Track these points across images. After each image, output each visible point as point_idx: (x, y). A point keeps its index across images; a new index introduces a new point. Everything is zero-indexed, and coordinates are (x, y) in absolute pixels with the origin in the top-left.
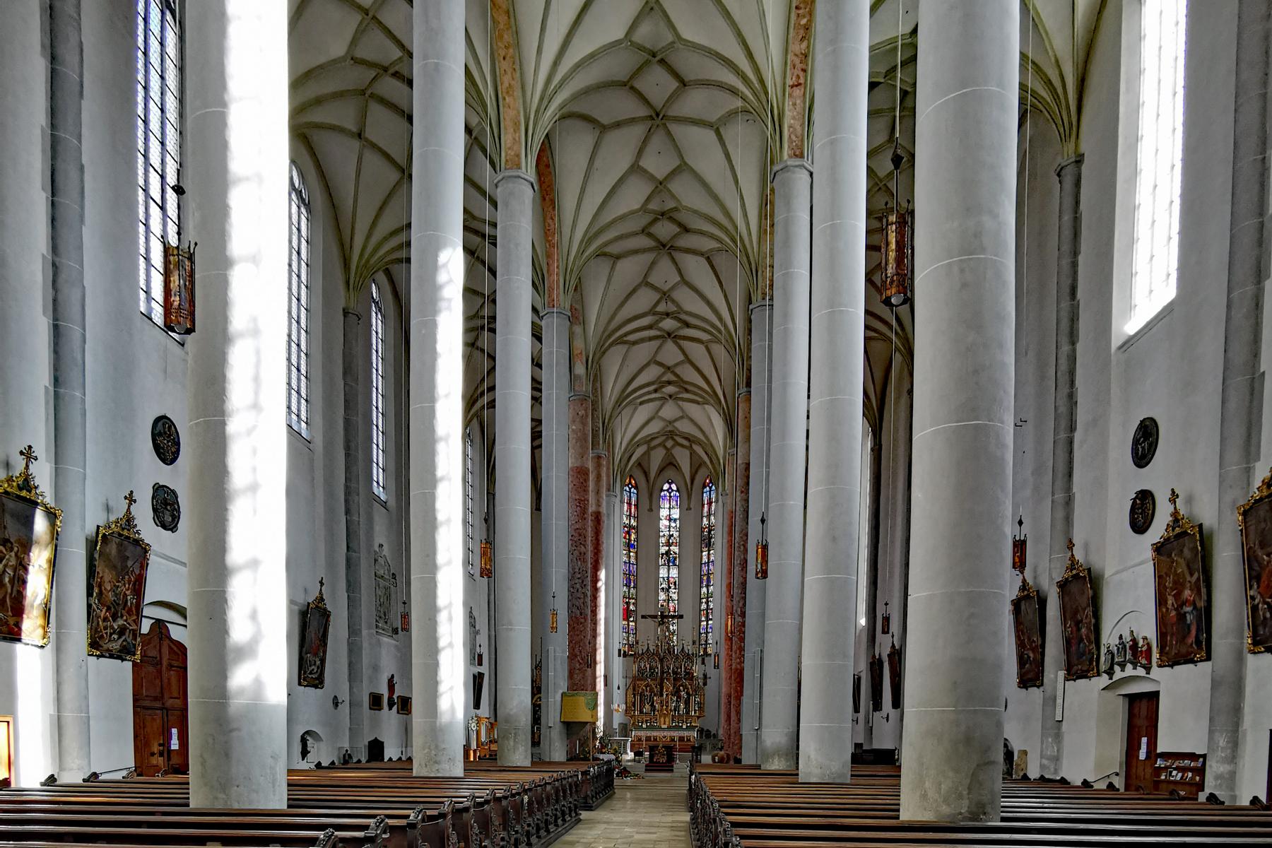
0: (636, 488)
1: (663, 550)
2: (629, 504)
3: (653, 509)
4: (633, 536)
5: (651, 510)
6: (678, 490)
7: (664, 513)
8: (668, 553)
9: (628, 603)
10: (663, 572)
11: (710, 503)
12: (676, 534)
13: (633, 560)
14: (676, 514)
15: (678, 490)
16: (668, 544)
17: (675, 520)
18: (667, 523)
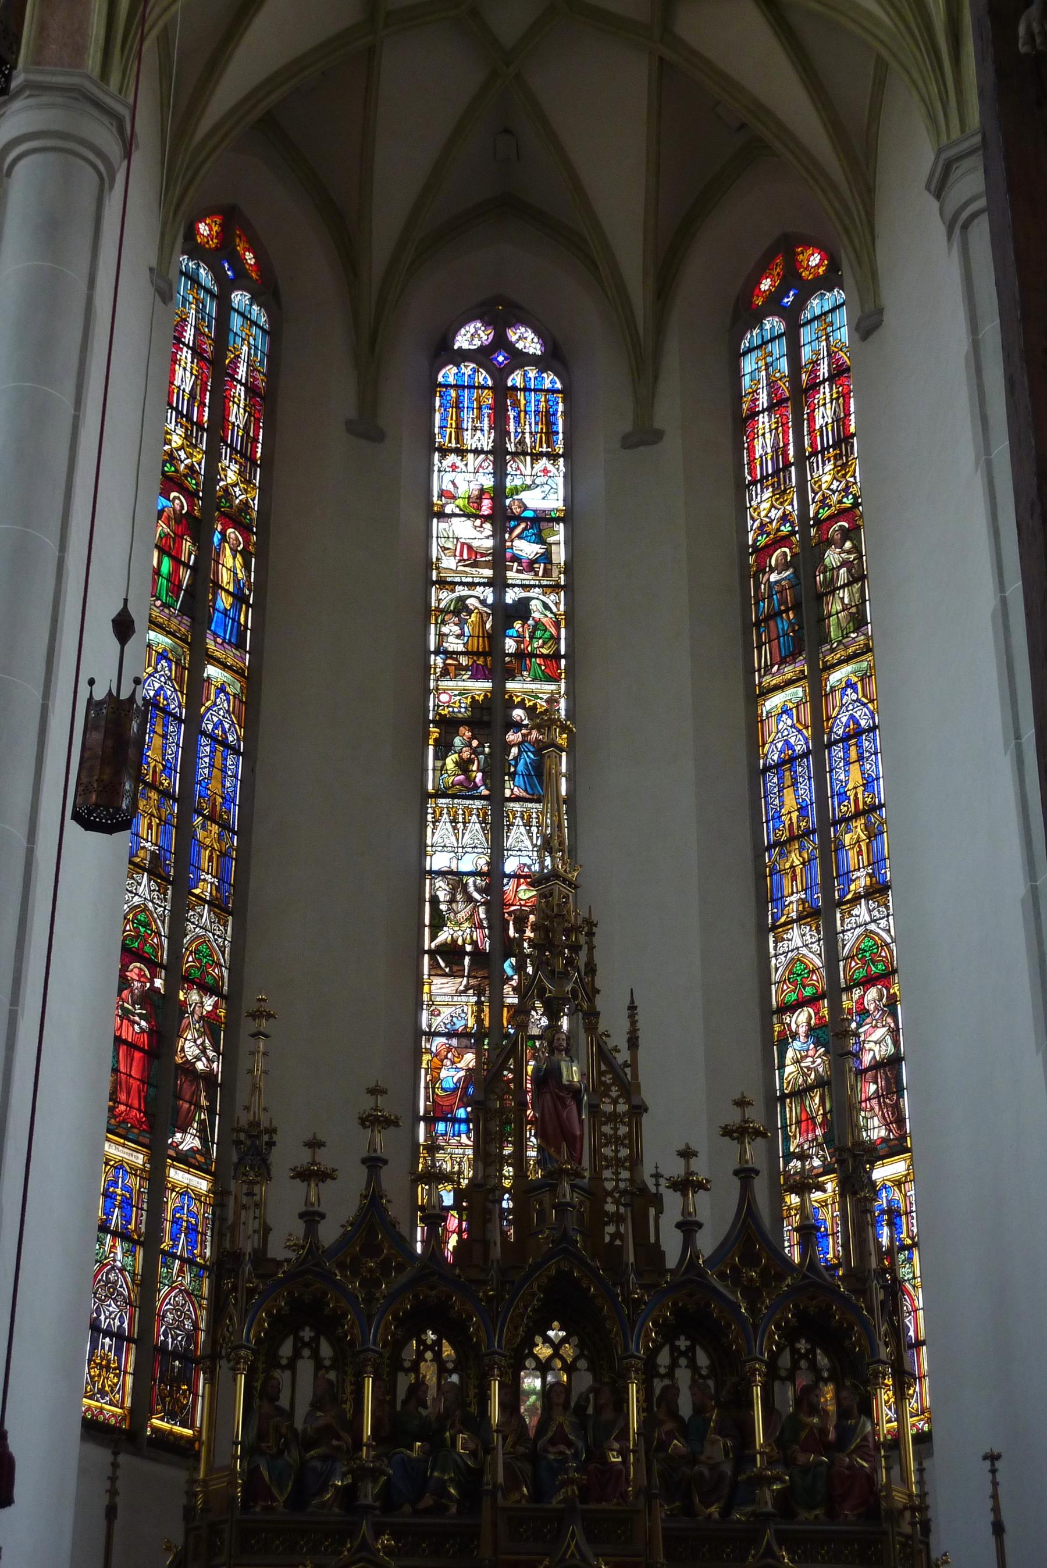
0: (266, 293)
1: (455, 693)
2: (215, 365)
3: (391, 436)
4: (230, 567)
5: (367, 427)
6: (552, 358)
7: (461, 478)
8: (488, 718)
9: (164, 1015)
10: (453, 847)
11: (795, 396)
12: (546, 606)
13: (218, 714)
14: (543, 489)
15: (552, 358)
16: (490, 660)
17: (539, 523)
18: (482, 538)
